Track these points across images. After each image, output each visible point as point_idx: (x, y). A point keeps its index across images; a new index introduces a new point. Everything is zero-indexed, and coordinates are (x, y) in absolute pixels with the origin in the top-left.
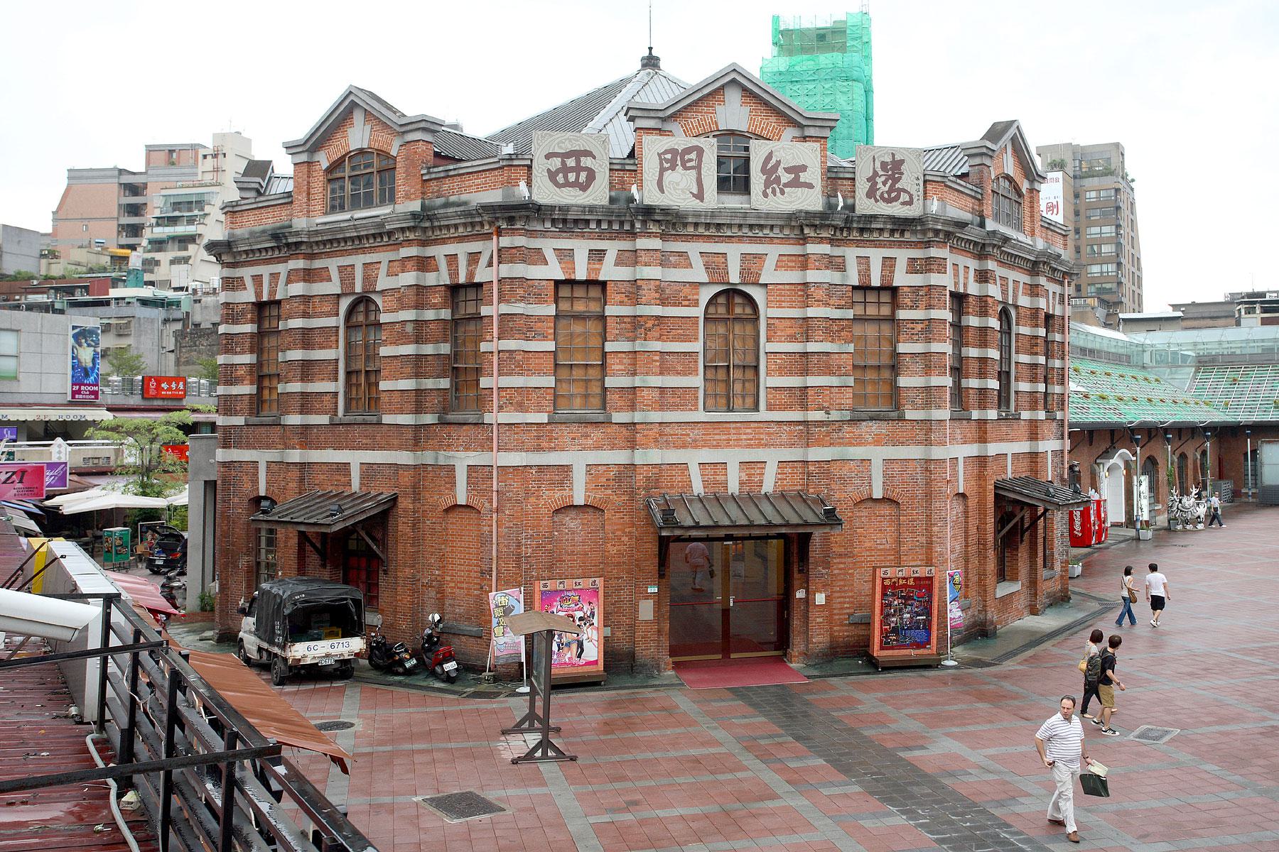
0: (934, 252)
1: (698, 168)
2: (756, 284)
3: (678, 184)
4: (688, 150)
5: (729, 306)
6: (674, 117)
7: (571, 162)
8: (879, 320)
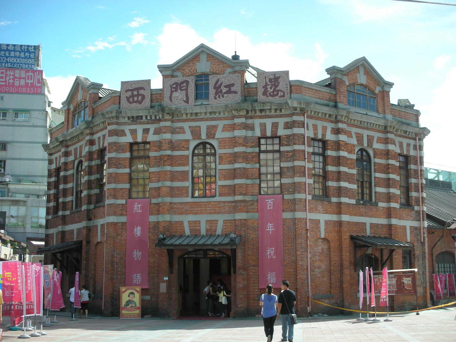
0: (295, 118)
1: (187, 90)
2: (213, 138)
3: (178, 97)
4: (182, 83)
6: (178, 69)
7: (135, 93)
8: (273, 152)
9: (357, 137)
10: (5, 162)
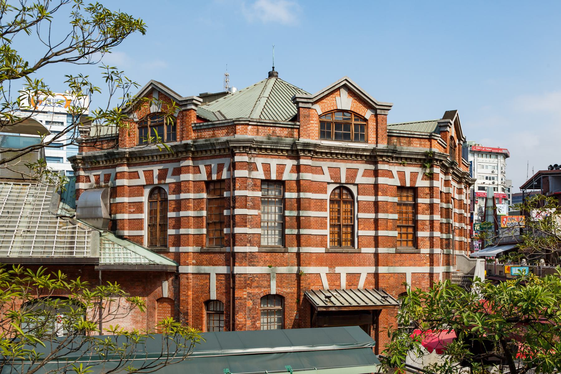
2: (354, 184)
5: (340, 195)
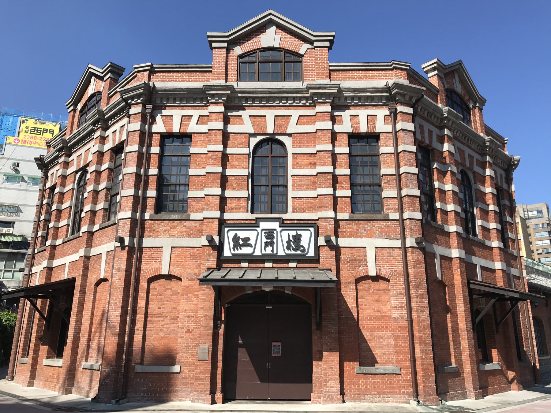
9: (460, 154)
10: (14, 223)
